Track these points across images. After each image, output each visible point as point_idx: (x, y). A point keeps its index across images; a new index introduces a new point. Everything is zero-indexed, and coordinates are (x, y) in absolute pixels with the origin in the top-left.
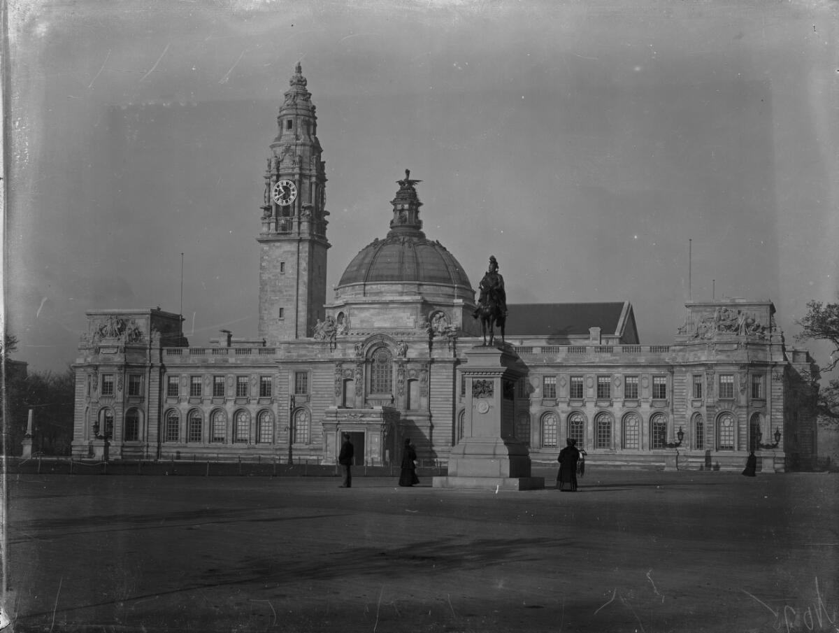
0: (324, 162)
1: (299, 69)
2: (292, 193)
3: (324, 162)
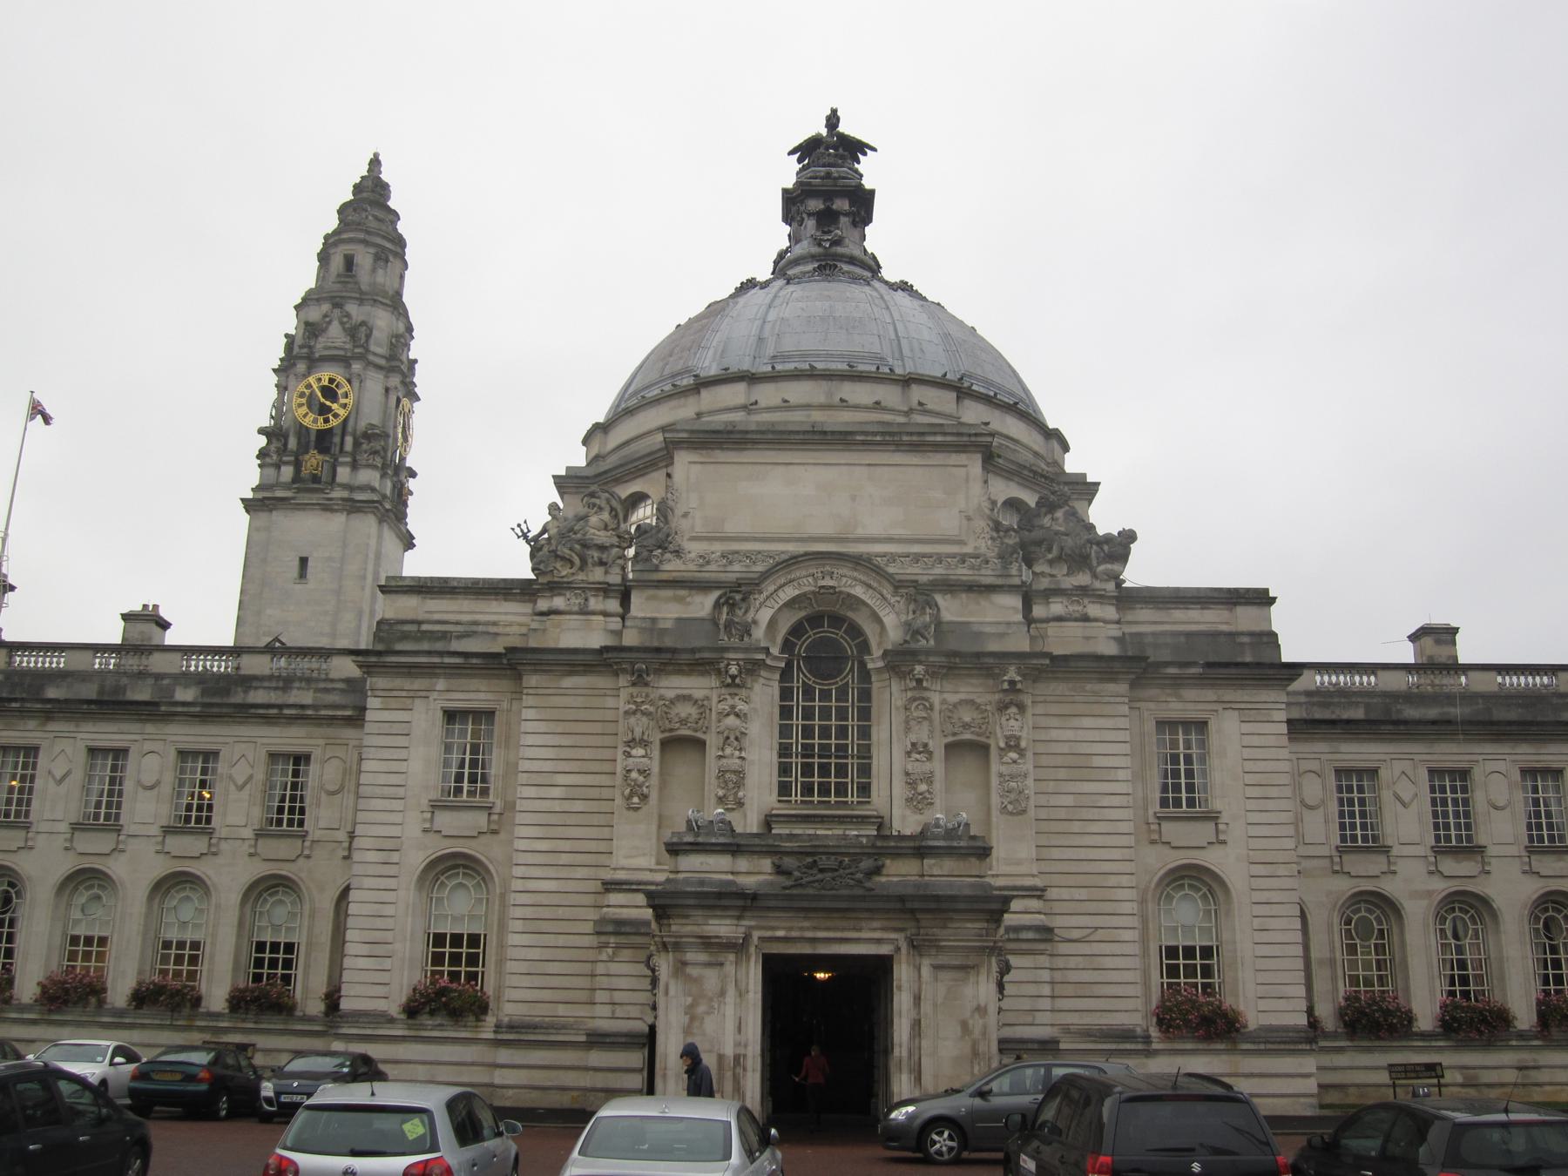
0: (415, 361)
1: (375, 163)
2: (343, 401)
3: (415, 361)
